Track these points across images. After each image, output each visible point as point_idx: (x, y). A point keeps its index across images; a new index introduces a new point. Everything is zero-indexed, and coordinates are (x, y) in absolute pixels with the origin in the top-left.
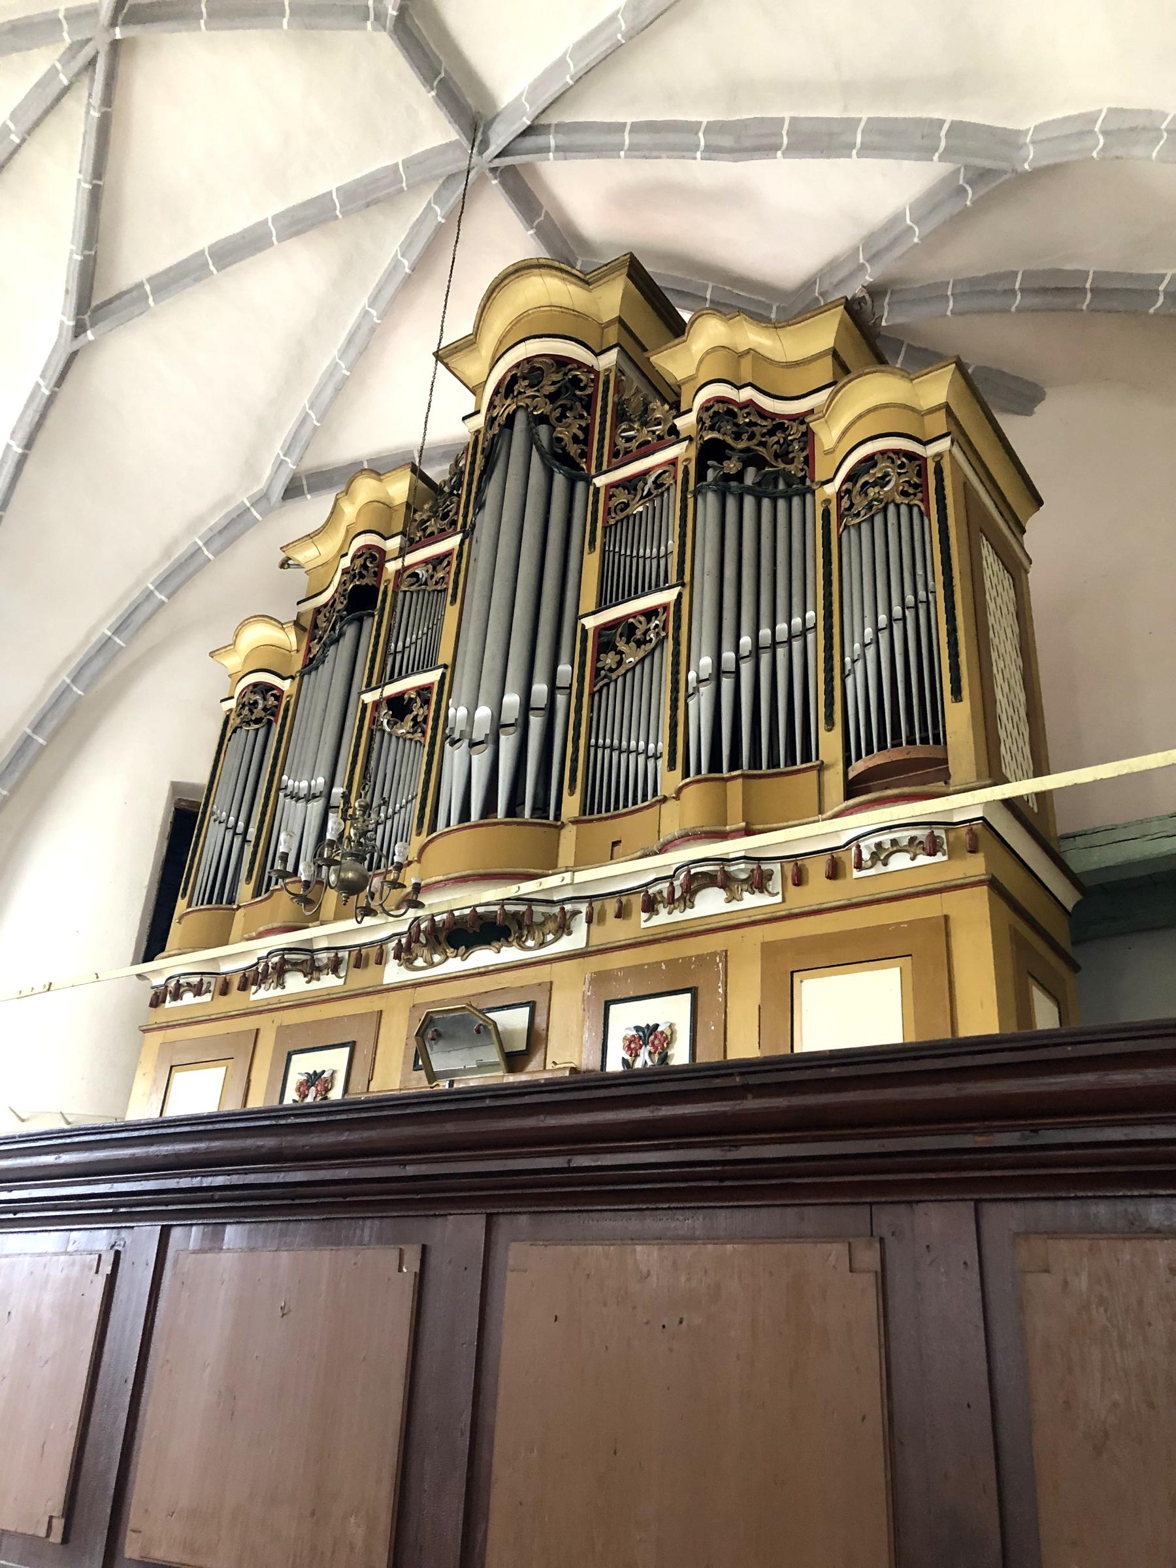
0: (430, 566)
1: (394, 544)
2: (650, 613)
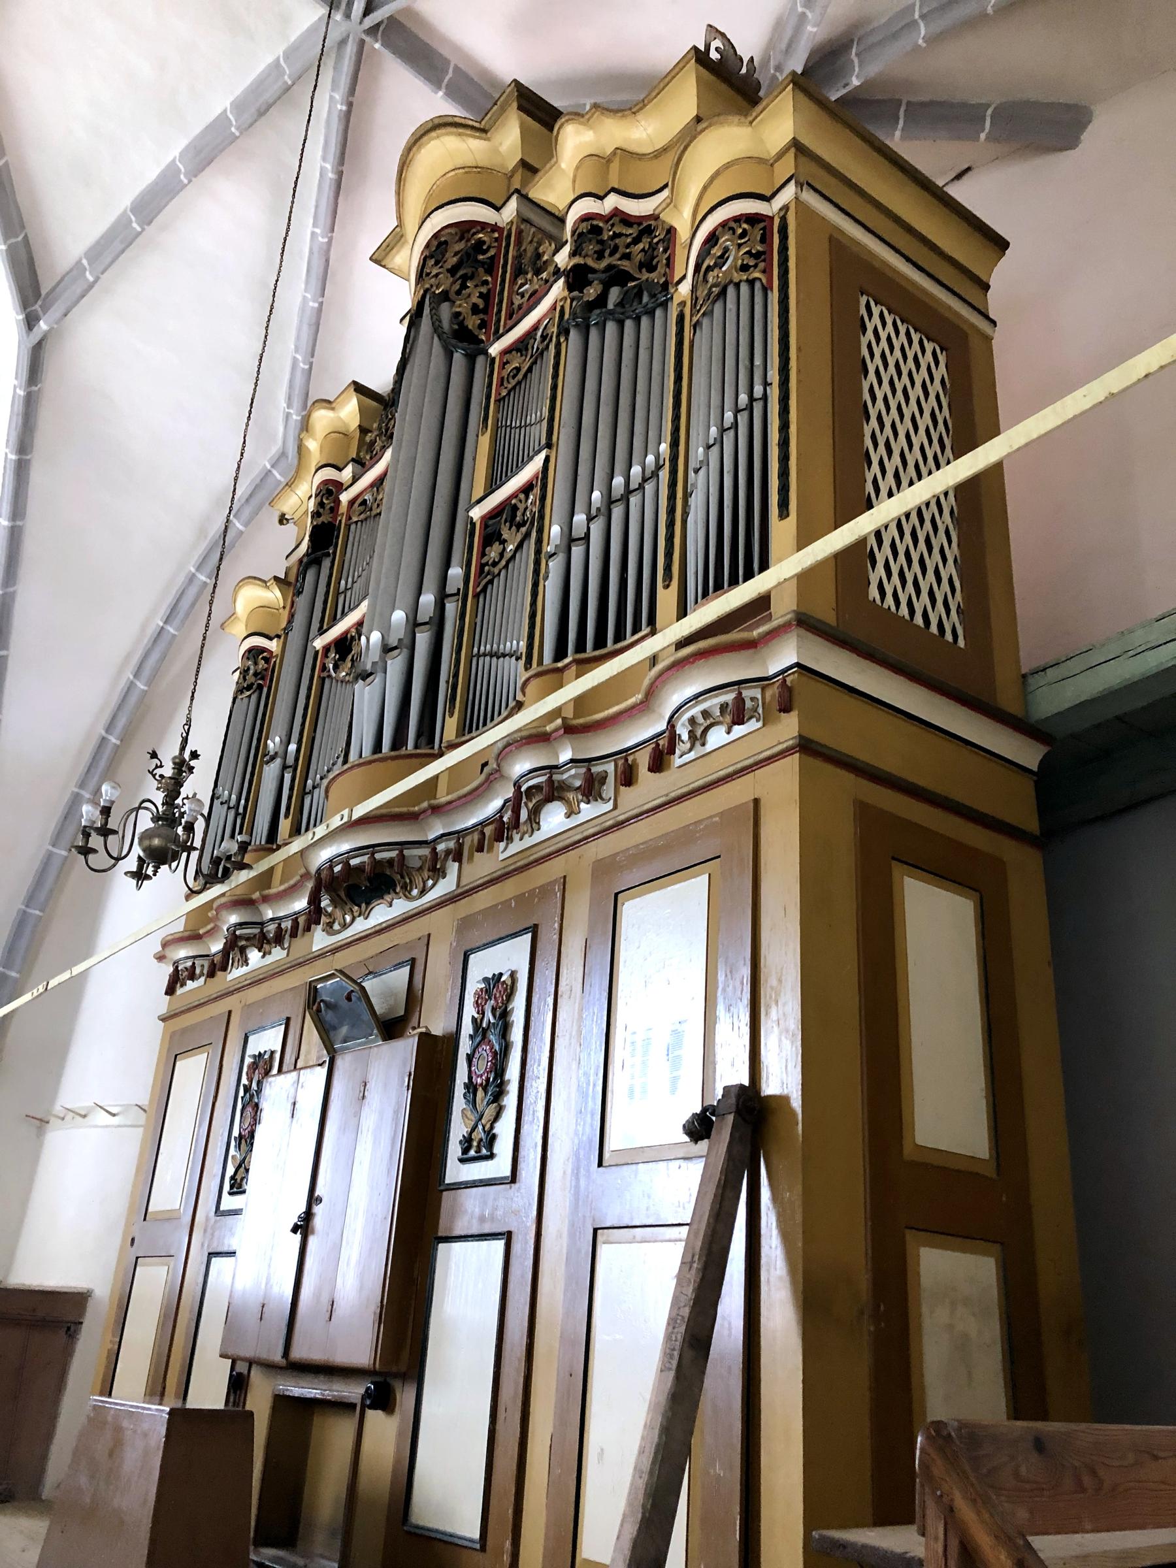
1: (347, 474)
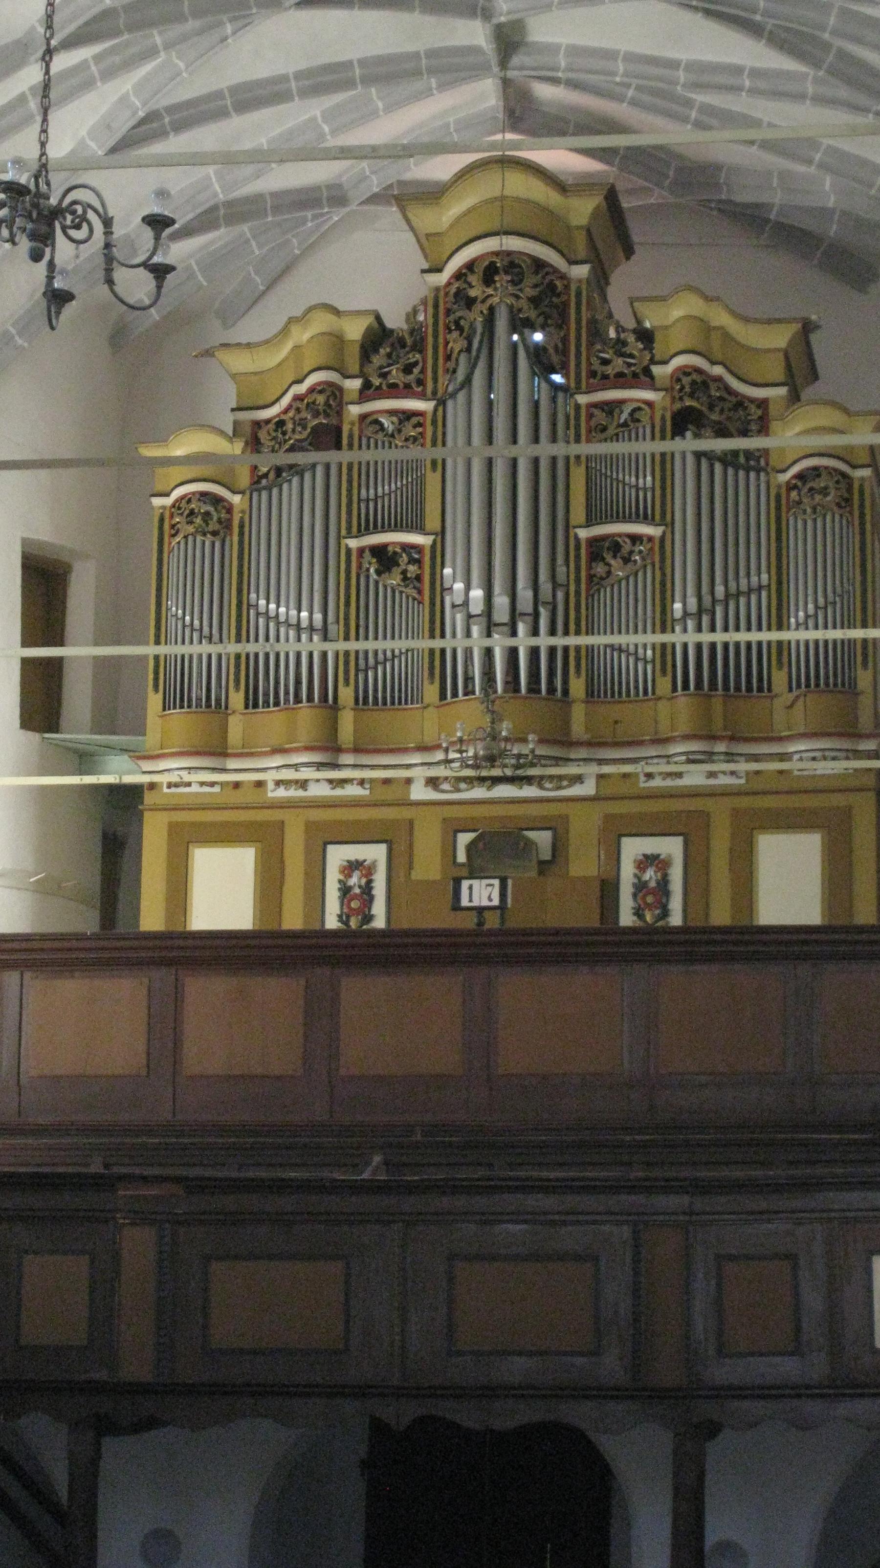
0: (395, 419)
1: (354, 385)
2: (635, 539)
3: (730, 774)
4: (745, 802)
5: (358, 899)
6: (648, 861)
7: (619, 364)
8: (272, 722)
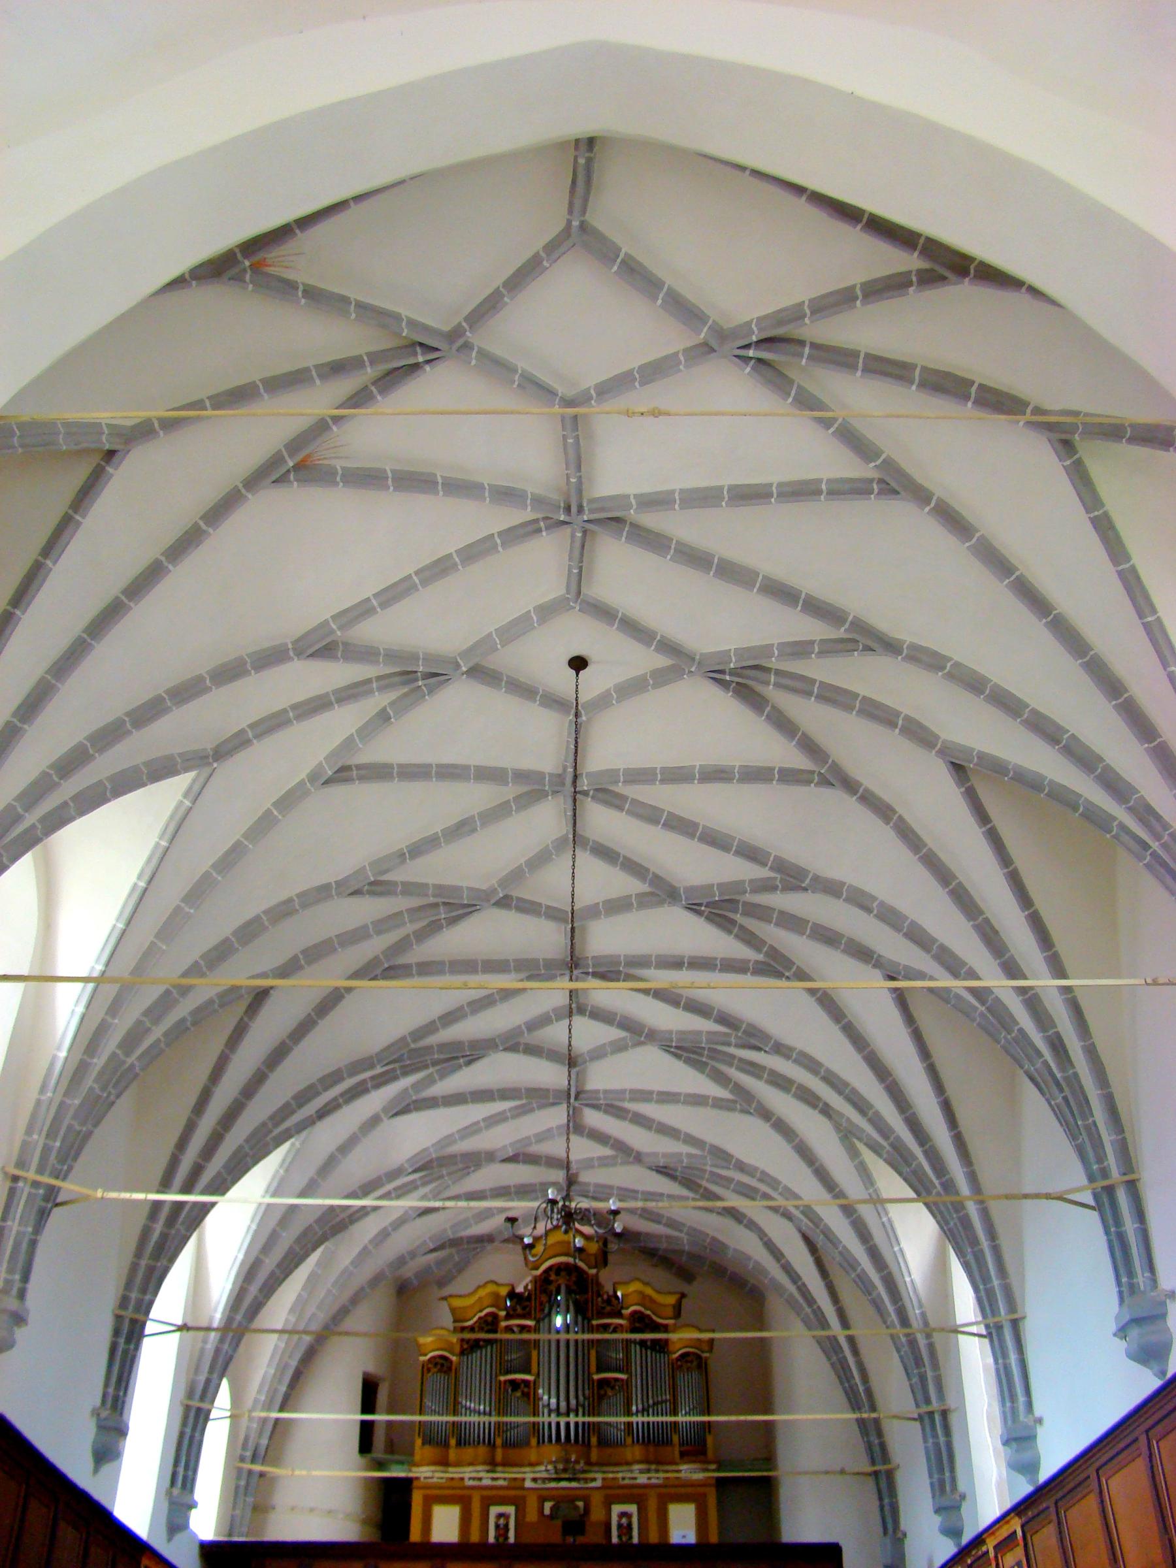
1: (503, 1313)
2: (616, 1380)
3: (657, 1477)
4: (664, 1490)
5: (502, 1530)
6: (623, 1515)
7: (608, 1308)
8: (469, 1452)
